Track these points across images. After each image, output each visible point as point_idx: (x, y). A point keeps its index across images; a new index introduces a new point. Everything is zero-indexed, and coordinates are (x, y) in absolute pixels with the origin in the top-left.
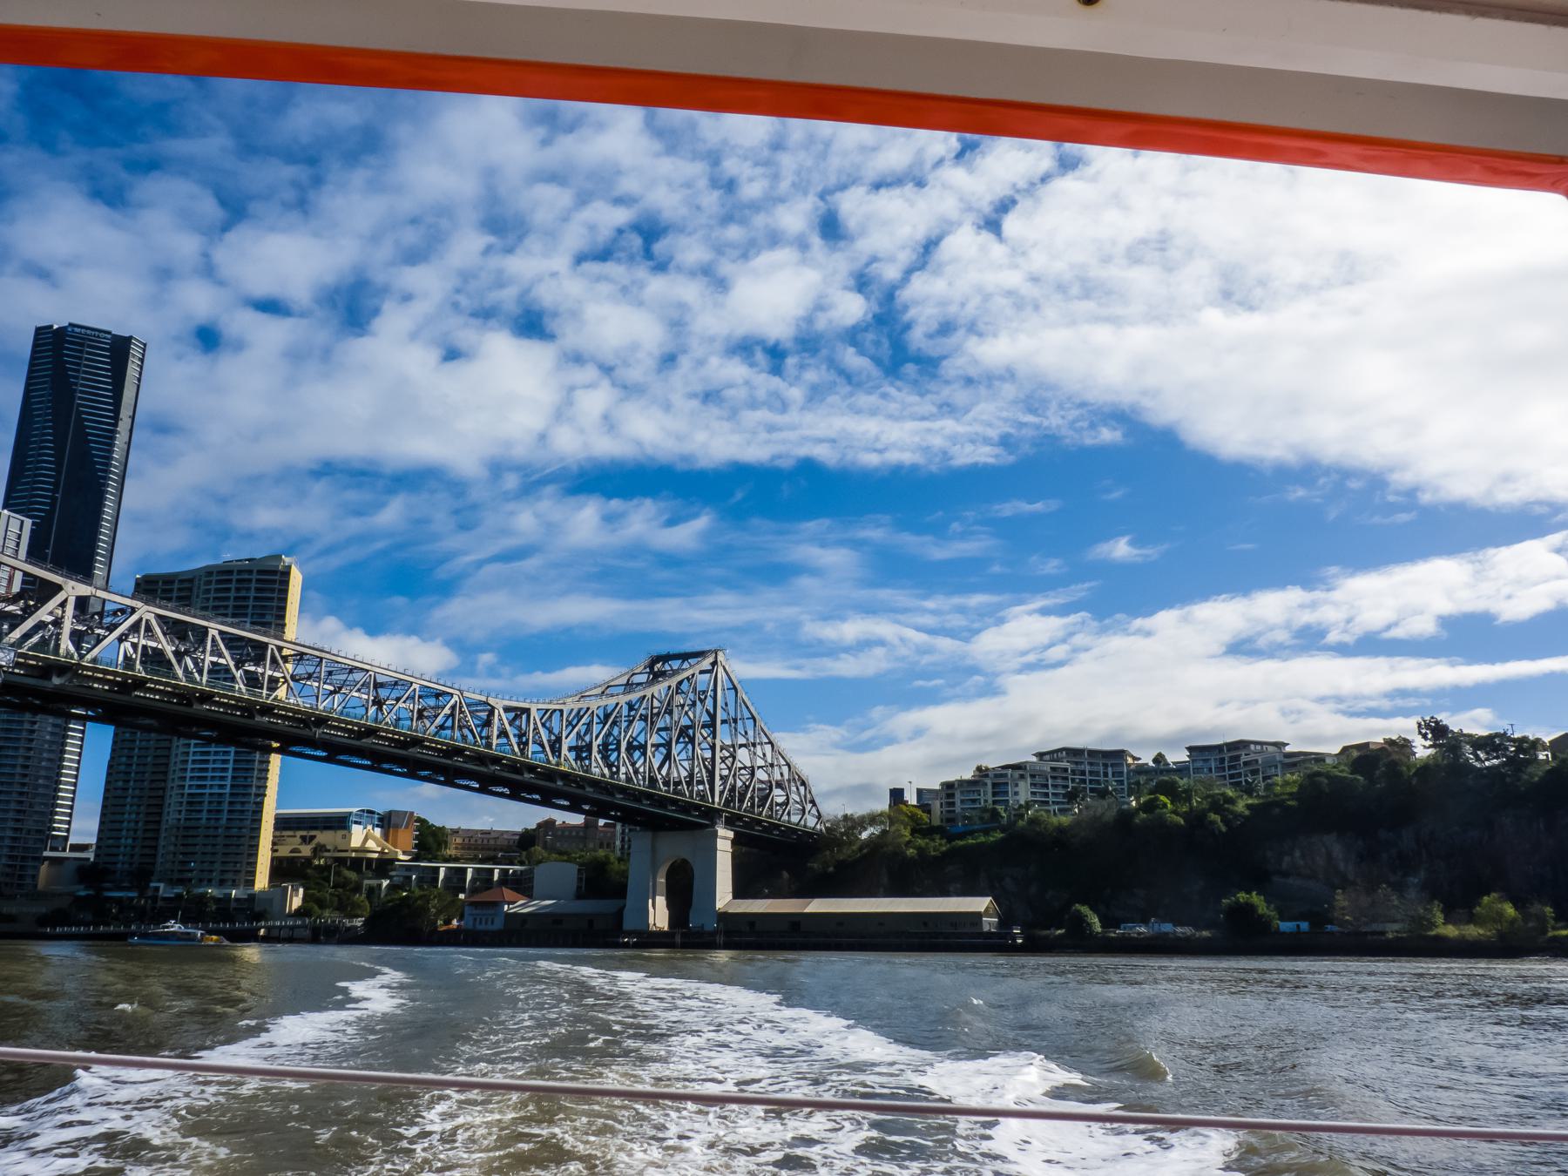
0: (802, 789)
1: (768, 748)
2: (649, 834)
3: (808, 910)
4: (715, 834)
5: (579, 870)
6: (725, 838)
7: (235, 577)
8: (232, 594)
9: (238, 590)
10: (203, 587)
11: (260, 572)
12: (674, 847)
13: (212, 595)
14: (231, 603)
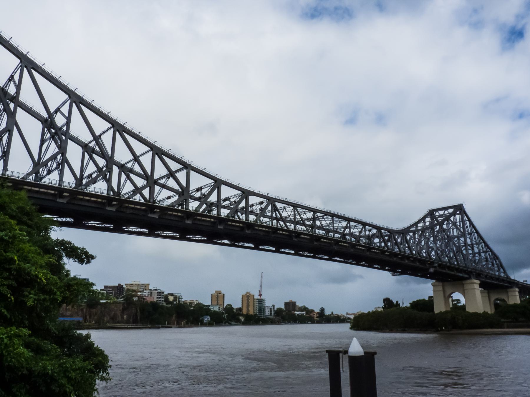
2: (441, 284)
4: (474, 283)
6: (477, 283)
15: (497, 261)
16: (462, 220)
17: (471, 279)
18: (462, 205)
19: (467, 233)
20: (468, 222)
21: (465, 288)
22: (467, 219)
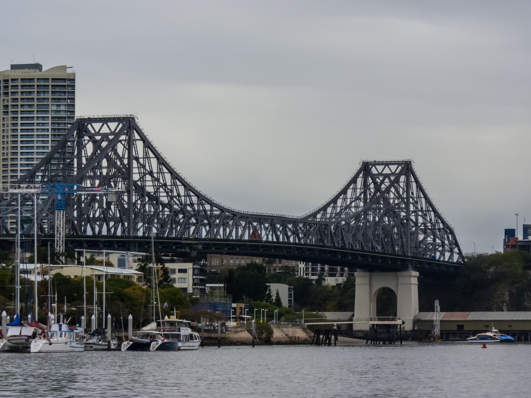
0: (450, 236)
1: (432, 213)
2: (368, 274)
3: (469, 318)
4: (411, 276)
5: (289, 288)
6: (415, 277)
7: (36, 83)
8: (35, 96)
9: (38, 92)
10: (10, 90)
13: (19, 96)
14: (35, 103)
15: (450, 236)
16: (408, 184)
18: (410, 162)
19: (411, 200)
20: (414, 185)
21: (398, 283)
22: (413, 180)
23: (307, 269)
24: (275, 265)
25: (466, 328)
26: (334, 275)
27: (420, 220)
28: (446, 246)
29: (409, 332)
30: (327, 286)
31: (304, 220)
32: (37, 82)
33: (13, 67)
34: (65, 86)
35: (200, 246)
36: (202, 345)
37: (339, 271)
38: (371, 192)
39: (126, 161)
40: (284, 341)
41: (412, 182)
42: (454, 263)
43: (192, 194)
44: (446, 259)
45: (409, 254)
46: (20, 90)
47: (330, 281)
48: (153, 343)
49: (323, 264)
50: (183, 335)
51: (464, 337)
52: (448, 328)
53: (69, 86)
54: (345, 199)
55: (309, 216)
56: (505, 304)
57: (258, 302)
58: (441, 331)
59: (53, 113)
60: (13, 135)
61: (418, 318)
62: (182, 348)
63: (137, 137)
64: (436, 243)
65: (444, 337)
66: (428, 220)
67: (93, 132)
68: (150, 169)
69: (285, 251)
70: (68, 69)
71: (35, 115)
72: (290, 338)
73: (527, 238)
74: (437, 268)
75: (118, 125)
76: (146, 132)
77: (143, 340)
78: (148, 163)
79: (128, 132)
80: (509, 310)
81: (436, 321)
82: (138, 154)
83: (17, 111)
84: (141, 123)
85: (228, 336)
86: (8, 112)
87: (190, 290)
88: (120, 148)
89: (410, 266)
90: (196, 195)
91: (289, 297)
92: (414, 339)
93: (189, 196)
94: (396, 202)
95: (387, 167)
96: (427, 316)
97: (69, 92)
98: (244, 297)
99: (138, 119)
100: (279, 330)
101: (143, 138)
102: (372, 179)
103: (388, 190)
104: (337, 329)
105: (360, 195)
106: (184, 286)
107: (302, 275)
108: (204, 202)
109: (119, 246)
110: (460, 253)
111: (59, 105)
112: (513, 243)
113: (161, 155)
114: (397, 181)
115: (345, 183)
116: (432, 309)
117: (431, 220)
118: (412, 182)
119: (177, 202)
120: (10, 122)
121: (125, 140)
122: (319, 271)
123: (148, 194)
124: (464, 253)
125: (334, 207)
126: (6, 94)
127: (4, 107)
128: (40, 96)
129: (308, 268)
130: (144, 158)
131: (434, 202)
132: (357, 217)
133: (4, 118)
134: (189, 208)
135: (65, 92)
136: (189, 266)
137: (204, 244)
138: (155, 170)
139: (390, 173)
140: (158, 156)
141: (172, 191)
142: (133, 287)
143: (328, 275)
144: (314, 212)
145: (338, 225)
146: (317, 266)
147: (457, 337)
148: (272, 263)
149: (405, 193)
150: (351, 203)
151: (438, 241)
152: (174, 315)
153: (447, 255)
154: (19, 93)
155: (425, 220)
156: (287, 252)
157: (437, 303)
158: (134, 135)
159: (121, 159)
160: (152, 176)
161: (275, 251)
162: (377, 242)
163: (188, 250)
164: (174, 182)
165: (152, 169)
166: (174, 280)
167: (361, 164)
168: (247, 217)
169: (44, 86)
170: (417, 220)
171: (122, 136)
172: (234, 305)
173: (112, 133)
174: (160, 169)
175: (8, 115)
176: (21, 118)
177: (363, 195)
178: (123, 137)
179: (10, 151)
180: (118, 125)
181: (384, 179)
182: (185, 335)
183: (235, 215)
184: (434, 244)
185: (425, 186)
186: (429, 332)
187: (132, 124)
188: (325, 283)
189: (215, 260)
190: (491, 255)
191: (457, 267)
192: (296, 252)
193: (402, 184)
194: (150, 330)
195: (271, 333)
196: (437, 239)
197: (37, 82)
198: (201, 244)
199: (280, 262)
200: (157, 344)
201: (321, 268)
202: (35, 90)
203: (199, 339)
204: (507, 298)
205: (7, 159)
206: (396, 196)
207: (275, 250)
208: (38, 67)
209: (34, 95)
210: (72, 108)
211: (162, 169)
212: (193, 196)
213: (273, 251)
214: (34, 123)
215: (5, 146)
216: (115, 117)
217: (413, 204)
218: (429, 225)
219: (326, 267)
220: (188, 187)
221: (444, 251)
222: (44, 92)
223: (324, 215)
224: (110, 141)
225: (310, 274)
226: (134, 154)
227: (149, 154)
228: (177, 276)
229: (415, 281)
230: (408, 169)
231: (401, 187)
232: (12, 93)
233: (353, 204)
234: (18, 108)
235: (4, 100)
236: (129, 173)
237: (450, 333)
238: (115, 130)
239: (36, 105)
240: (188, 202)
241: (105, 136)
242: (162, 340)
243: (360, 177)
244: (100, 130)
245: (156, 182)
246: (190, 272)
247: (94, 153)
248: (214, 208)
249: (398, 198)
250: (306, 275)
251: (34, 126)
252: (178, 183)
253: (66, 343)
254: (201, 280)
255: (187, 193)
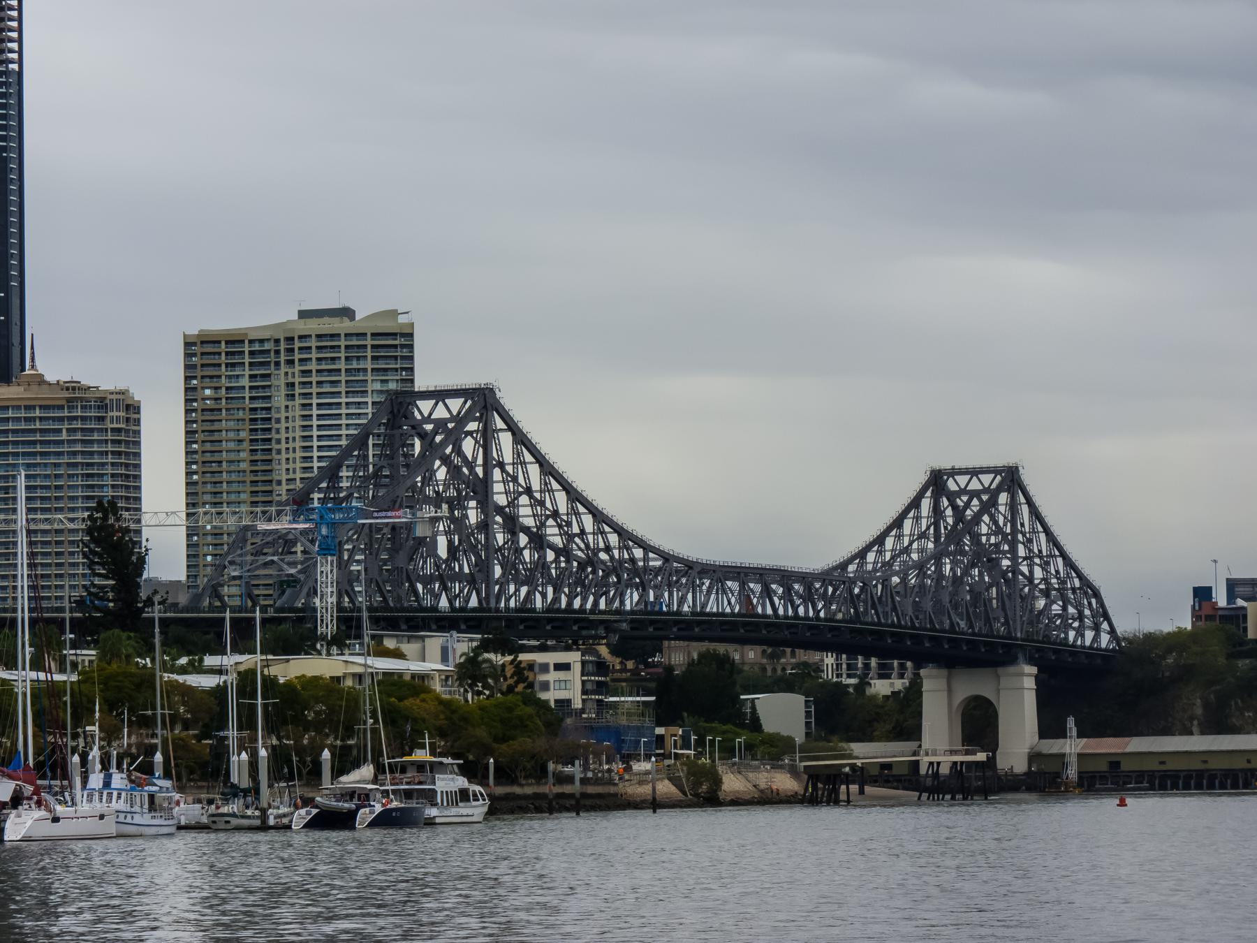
0: (1094, 601)
1: (1060, 560)
2: (944, 672)
3: (1128, 750)
4: (1023, 674)
5: (806, 701)
6: (1029, 675)
7: (343, 343)
8: (342, 365)
9: (347, 358)
10: (297, 356)
11: (375, 335)
12: (971, 685)
13: (313, 366)
14: (343, 378)
15: (1094, 601)
16: (1013, 507)
17: (1018, 664)
19: (1020, 537)
20: (1025, 509)
22: (1023, 500)
23: (839, 666)
24: (783, 660)
25: (1126, 766)
26: (888, 677)
27: (1038, 573)
28: (1086, 620)
29: (1021, 775)
30: (874, 697)
31: (826, 577)
32: (346, 340)
33: (303, 314)
34: (395, 346)
35: (625, 624)
36: (492, 812)
37: (896, 669)
38: (947, 523)
39: (480, 471)
40: (748, 797)
41: (1020, 504)
42: (1101, 650)
43: (607, 529)
44: (1088, 643)
45: (1019, 635)
46: (314, 355)
47: (881, 687)
48: (362, 811)
49: (867, 656)
50: (442, 792)
51: (1121, 783)
52: (1091, 767)
53: (403, 346)
54: (899, 537)
55: (835, 568)
56: (1195, 722)
57: (713, 725)
58: (1079, 773)
59: (375, 395)
60: (303, 437)
61: (1037, 749)
62: (438, 820)
63: (500, 424)
64: (1067, 613)
65: (1086, 783)
66: (1053, 572)
67: (419, 417)
68: (526, 484)
69: (786, 633)
70: (400, 316)
71: (344, 400)
72: (762, 791)
73: (1234, 603)
74: (1070, 660)
75: (465, 402)
76: (517, 415)
77: (340, 804)
78: (523, 472)
79: (482, 415)
80: (1203, 733)
81: (1070, 754)
82: (502, 456)
83: (311, 394)
84: (507, 399)
85: (623, 791)
86: (293, 395)
87: (578, 704)
88: (468, 446)
89: (1021, 656)
90: (615, 531)
91: (806, 718)
92: (1030, 789)
93: (603, 533)
94: (993, 540)
95: (975, 478)
96: (1053, 746)
97: (403, 358)
98: (685, 714)
99: (500, 391)
100: (739, 777)
101: (512, 427)
102: (949, 500)
103: (977, 519)
104: (850, 773)
105: (928, 528)
106: (562, 695)
107: (830, 677)
108: (631, 543)
109: (469, 627)
110: (1112, 631)
111: (386, 381)
112: (1210, 612)
113: (547, 457)
114: (993, 502)
115: (900, 508)
116: (1062, 734)
117: (1057, 572)
118: (1020, 504)
119: (582, 546)
120: (298, 412)
121: (477, 431)
122: (860, 670)
123: (526, 530)
124: (1119, 631)
125: (880, 552)
126: (290, 362)
127: (288, 387)
128: (352, 364)
129: (841, 664)
130: (513, 464)
131: (1062, 540)
132: (921, 566)
133: (287, 407)
134: (603, 556)
135: (396, 358)
136: (574, 657)
137: (632, 621)
138: (536, 486)
139: (982, 488)
140: (541, 461)
141: (569, 524)
142: (423, 696)
143: (876, 676)
144: (842, 560)
145: (886, 583)
146: (857, 659)
147: (1109, 783)
148: (779, 658)
149: (1009, 524)
150: (911, 543)
151: (1071, 610)
152: (425, 748)
153: (1089, 635)
154: (314, 360)
155: (1047, 572)
156: (790, 633)
157: (1071, 722)
158: (495, 421)
159: (471, 465)
160: (531, 497)
161: (768, 632)
162: (960, 616)
163: (603, 632)
164: (572, 507)
165: (530, 484)
166: (545, 686)
167: (928, 473)
168: (714, 571)
169: (359, 347)
170: (1031, 572)
171: (471, 423)
172: (660, 731)
173: (453, 418)
174: (546, 484)
175: (294, 400)
176: (318, 405)
177: (932, 528)
178: (472, 426)
179: (299, 465)
180: (465, 402)
181: (970, 500)
182: (447, 792)
183: (691, 568)
184: (1064, 616)
185: (1044, 511)
186: (1058, 775)
187: (489, 401)
188: (870, 691)
189: (677, 656)
190: (1169, 634)
191: (1106, 655)
192: (808, 634)
193: (1002, 509)
194: (358, 782)
195: (717, 782)
196: (1069, 607)
197: (346, 340)
198: (626, 621)
199: (793, 654)
200: (372, 812)
201: (863, 663)
202: (343, 355)
203: (484, 800)
204: (1199, 711)
205: (295, 479)
206: (992, 530)
207: (769, 629)
208: (347, 313)
209: (340, 364)
210: (410, 385)
211: (550, 484)
212: (610, 533)
213: (764, 632)
214: (340, 415)
215: (291, 455)
216: (459, 387)
217: (1023, 543)
218: (1054, 581)
219: (874, 662)
220: (599, 516)
221: (1084, 627)
222: (358, 358)
223: (861, 565)
224: (449, 433)
225: (844, 676)
226: (495, 455)
227: (523, 456)
228: (552, 676)
229: (1030, 683)
230: (1012, 481)
231: (1002, 514)
232: (300, 360)
233: (915, 545)
234: (311, 387)
235: (286, 374)
236: (487, 492)
237: (1095, 776)
238: (459, 413)
239: (343, 382)
240: (602, 545)
241: (440, 424)
242: (383, 805)
243: (927, 497)
244: (430, 414)
245: (539, 508)
246: (577, 668)
247: (422, 454)
248: (651, 555)
249: (996, 534)
250: (837, 677)
251: (341, 419)
252: (581, 509)
253: (102, 817)
254: (598, 683)
255: (599, 529)
